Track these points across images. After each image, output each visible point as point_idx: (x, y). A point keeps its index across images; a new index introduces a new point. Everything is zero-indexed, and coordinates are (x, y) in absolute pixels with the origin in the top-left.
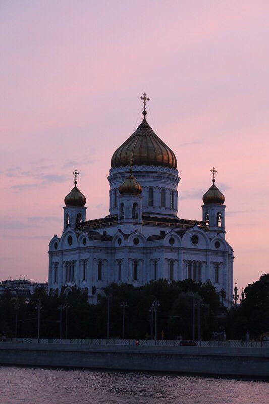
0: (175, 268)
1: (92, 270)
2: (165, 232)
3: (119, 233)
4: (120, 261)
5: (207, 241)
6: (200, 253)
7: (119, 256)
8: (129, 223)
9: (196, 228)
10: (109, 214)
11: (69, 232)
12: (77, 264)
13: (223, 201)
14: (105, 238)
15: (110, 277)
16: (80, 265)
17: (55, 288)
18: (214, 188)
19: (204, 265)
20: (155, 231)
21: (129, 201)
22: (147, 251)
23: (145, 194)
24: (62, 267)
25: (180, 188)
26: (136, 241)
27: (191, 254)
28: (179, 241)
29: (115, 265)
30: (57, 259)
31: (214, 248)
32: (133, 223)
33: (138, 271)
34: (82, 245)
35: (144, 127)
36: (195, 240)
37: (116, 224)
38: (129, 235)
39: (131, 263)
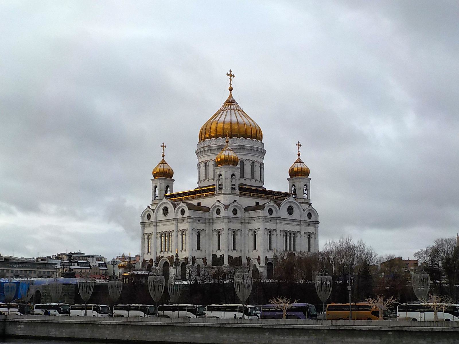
0: (273, 237)
1: (190, 241)
2: (259, 203)
3: (218, 204)
5: (301, 212)
6: (295, 223)
7: (218, 226)
10: (197, 186)
11: (164, 203)
12: (174, 234)
14: (199, 207)
15: (209, 248)
16: (178, 236)
17: (148, 258)
18: (299, 161)
19: (298, 235)
20: (250, 202)
22: (244, 221)
24: (157, 238)
25: (266, 161)
26: (235, 212)
27: (288, 224)
28: (276, 211)
29: (213, 235)
30: (149, 230)
33: (236, 242)
34: (180, 215)
36: (290, 210)
37: (213, 195)
38: (229, 205)
39: (231, 233)
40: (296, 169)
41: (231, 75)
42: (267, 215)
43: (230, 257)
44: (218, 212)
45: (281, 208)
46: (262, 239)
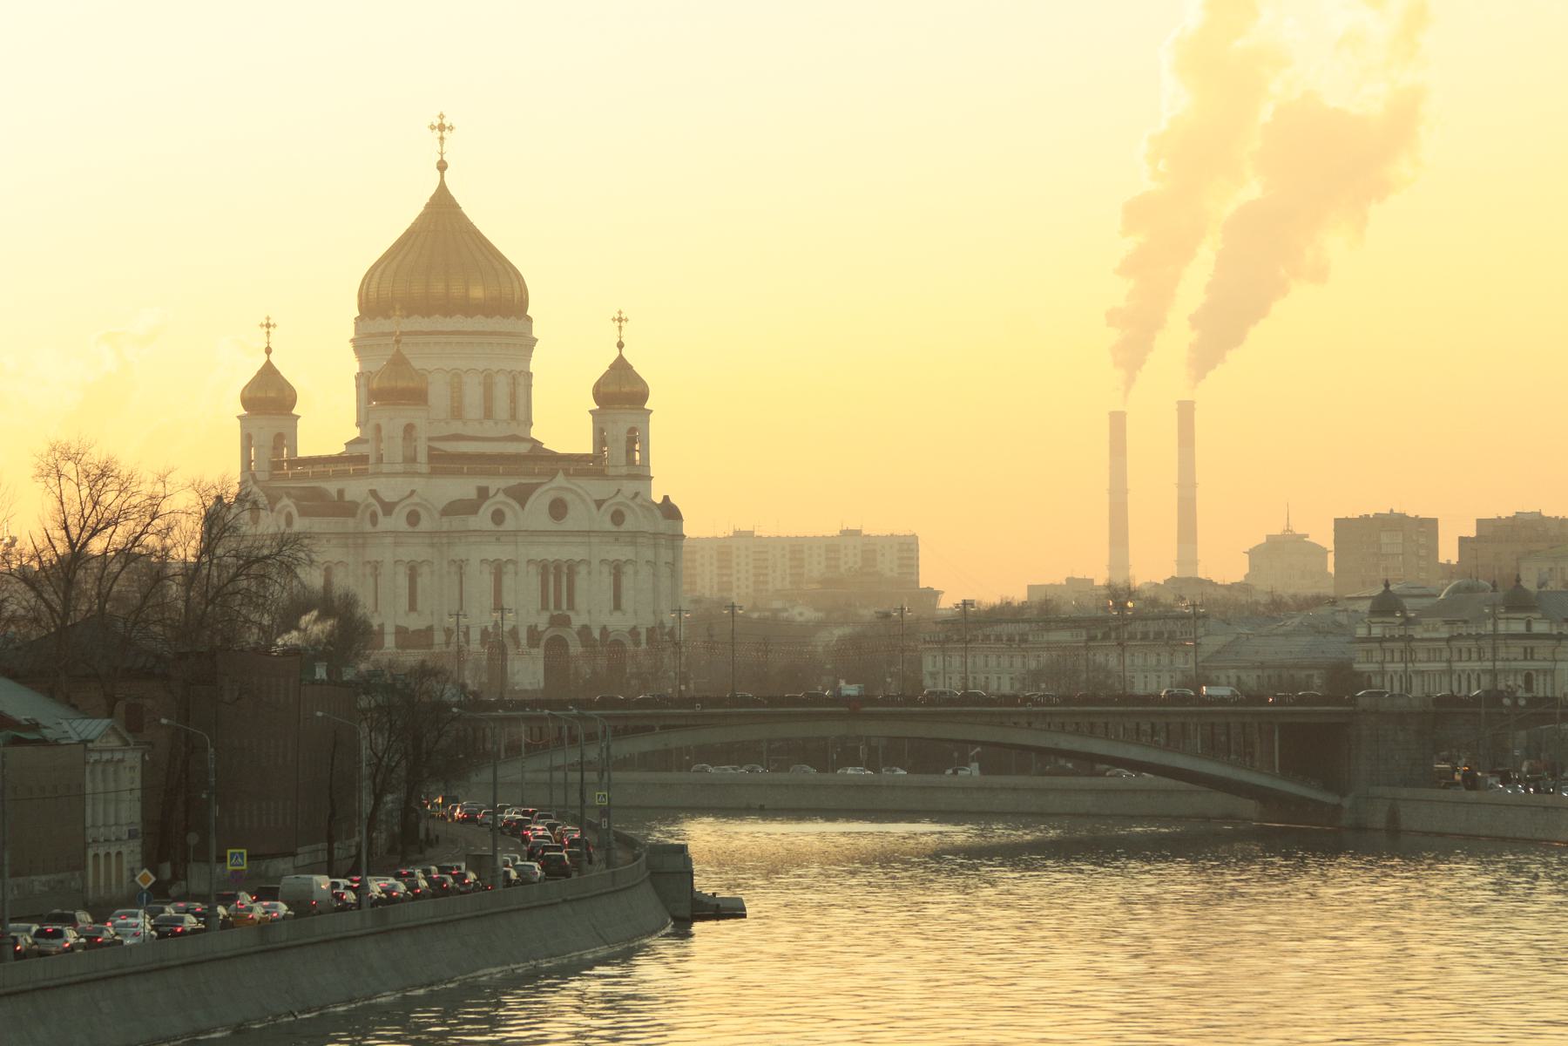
0: (508, 581)
3: (372, 500)
4: (376, 566)
8: (396, 474)
9: (560, 480)
10: (355, 433)
13: (643, 396)
19: (583, 570)
21: (394, 420)
23: (439, 394)
25: (538, 363)
26: (413, 518)
31: (609, 526)
32: (405, 474)
33: (419, 591)
35: (443, 208)
36: (558, 509)
39: (402, 571)
40: (612, 388)
41: (442, 128)
42: (490, 526)
43: (400, 632)
44: (374, 516)
45: (528, 506)
46: (480, 584)
